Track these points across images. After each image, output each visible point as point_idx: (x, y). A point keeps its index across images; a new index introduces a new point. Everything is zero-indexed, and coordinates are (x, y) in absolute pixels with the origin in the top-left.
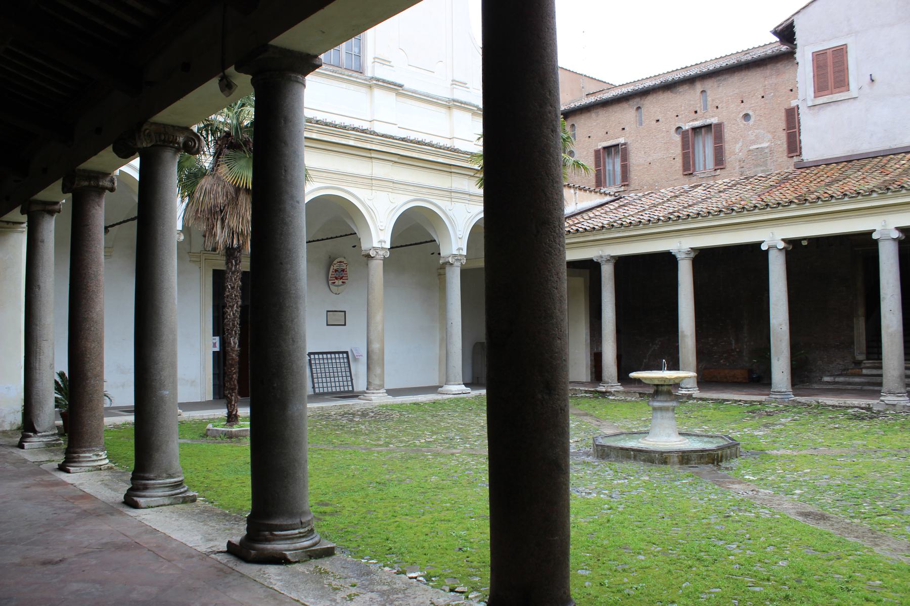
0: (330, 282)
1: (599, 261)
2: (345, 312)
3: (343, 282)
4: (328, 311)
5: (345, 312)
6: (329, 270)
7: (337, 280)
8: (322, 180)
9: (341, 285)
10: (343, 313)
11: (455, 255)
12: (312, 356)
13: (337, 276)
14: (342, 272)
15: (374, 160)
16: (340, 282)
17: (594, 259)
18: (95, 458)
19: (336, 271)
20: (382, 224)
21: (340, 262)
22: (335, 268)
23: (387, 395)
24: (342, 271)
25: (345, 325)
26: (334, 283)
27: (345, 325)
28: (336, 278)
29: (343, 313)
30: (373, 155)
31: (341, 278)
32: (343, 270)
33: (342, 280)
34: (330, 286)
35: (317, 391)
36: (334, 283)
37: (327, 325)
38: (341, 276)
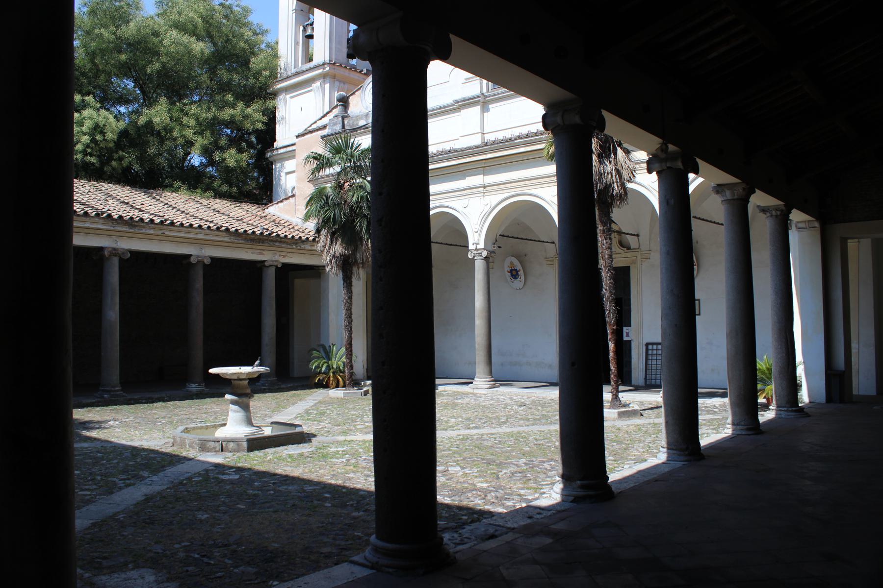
35: (648, 383)
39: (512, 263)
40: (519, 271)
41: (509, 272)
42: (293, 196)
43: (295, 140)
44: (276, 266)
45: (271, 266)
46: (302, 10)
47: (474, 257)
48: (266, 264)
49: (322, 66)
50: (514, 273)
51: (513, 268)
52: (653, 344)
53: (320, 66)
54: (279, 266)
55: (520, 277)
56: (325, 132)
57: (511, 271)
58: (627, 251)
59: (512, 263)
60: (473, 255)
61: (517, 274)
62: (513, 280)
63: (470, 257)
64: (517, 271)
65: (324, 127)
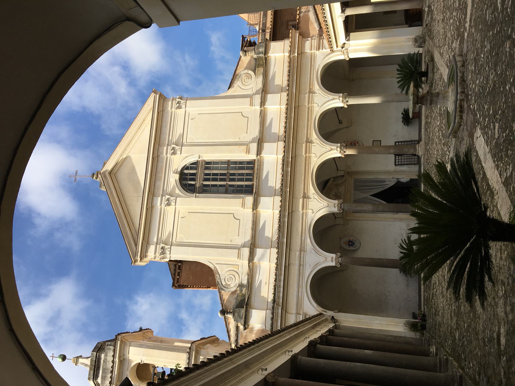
1: (345, 17)
2: (373, 141)
3: (357, 143)
5: (373, 141)
8: (309, 183)
10: (374, 142)
14: (352, 144)
15: (296, 155)
17: (343, 20)
18: (432, 354)
20: (328, 149)
23: (419, 144)
25: (380, 141)
27: (380, 141)
29: (374, 142)
33: (356, 144)
38: (354, 144)
39: (344, 243)
40: (350, 240)
41: (350, 247)
47: (342, 209)
49: (191, 350)
50: (350, 243)
51: (348, 243)
55: (353, 240)
56: (241, 327)
57: (349, 245)
58: (345, 177)
59: (344, 243)
60: (341, 209)
61: (351, 241)
62: (354, 246)
64: (349, 241)
65: (237, 328)
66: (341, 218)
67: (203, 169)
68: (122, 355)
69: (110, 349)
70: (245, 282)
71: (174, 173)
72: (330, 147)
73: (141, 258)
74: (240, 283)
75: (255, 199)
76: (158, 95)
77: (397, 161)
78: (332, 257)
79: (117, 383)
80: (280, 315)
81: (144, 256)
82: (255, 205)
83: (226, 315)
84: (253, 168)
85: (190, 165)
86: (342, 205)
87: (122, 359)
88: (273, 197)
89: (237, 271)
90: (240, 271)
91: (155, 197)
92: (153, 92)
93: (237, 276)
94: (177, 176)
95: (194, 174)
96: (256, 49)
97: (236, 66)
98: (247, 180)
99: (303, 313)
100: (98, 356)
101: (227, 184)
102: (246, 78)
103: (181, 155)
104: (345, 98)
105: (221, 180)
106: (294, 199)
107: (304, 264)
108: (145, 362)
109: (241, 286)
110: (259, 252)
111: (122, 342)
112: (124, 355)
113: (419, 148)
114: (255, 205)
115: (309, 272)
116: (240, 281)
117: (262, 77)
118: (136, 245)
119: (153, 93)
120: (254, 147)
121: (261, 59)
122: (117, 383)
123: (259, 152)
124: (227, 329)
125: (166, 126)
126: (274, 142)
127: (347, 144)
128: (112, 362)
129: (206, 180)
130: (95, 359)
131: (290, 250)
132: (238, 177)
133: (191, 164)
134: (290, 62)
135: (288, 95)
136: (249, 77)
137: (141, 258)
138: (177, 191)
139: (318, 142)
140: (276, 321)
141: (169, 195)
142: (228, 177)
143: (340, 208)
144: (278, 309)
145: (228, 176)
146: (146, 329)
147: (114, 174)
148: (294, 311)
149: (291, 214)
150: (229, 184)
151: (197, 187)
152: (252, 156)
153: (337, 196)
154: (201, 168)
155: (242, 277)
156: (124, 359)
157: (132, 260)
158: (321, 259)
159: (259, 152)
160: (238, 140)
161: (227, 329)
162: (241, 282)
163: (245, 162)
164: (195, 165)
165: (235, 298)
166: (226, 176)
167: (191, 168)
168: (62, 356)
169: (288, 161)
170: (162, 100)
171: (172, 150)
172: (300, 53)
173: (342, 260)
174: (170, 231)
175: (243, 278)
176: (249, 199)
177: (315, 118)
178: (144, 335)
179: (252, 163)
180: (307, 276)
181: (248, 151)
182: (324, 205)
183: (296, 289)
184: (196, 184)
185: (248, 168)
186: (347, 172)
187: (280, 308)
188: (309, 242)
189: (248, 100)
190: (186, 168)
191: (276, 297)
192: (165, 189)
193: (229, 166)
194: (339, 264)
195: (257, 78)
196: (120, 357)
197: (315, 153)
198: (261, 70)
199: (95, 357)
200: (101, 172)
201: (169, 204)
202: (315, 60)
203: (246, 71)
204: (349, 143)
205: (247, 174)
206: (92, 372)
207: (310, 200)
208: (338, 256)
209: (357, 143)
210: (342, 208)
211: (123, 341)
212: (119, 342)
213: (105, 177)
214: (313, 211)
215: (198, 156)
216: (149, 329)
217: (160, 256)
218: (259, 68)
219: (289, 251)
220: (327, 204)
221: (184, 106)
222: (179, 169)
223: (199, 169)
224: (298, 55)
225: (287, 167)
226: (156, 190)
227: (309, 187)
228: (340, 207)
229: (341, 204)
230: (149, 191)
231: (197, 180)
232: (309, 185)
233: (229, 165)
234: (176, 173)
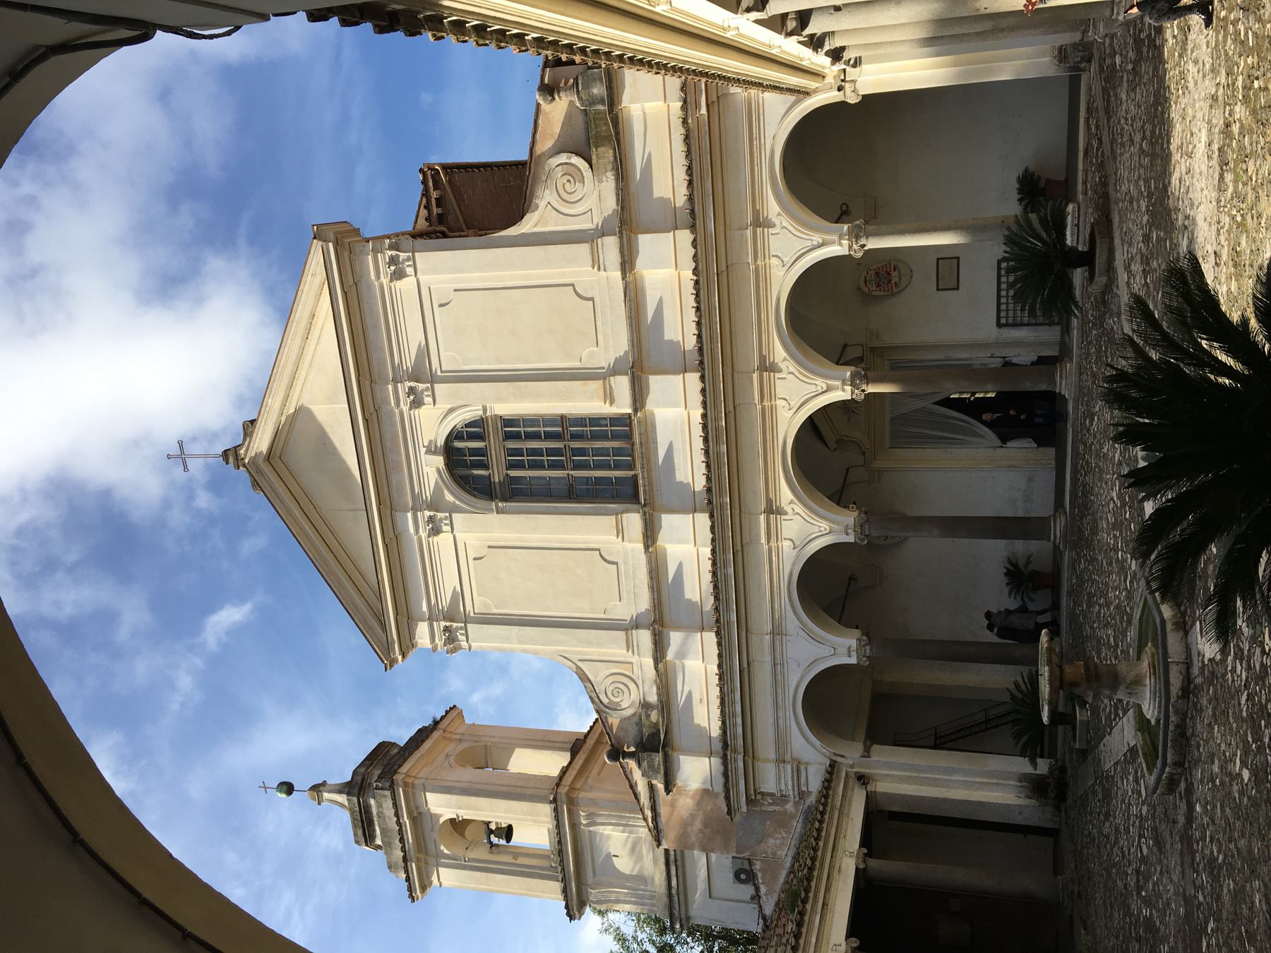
0: (895, 290)
2: (938, 259)
3: (894, 270)
4: (938, 289)
5: (938, 259)
6: (879, 296)
7: (891, 281)
9: (900, 272)
11: (850, 247)
12: (1003, 321)
13: (886, 282)
14: (881, 276)
15: (737, 403)
16: (894, 274)
19: (878, 285)
20: (819, 388)
21: (866, 282)
22: (874, 288)
24: (878, 276)
25: (958, 258)
26: (895, 283)
27: (958, 258)
28: (890, 281)
30: (731, 408)
31: (889, 274)
32: (877, 274)
34: (900, 288)
36: (895, 283)
37: (958, 288)
38: (886, 275)
42: (750, 862)
43: (661, 851)
44: (866, 855)
45: (864, 862)
46: (467, 849)
48: (861, 867)
52: (998, 317)
53: (556, 810)
54: (866, 851)
56: (660, 786)
63: (866, 542)
65: (651, 788)
66: (861, 466)
67: (501, 439)
68: (414, 809)
69: (385, 796)
70: (653, 698)
71: (429, 452)
72: (826, 383)
73: (403, 653)
74: (642, 700)
75: (648, 521)
76: (331, 245)
77: (1003, 314)
78: (849, 647)
79: (419, 855)
80: (741, 771)
81: (408, 647)
82: (650, 534)
83: (621, 760)
84: (628, 437)
85: (466, 427)
86: (866, 526)
87: (416, 815)
88: (672, 232)
89: (631, 674)
90: (637, 674)
91: (377, 385)
92: (315, 238)
93: (632, 685)
94: (439, 461)
95: (481, 452)
96: (580, 89)
97: (531, 135)
98: (618, 466)
99: (793, 760)
100: (363, 803)
101: (570, 477)
102: (569, 181)
103: (436, 406)
104: (857, 238)
105: (553, 466)
106: (743, 516)
107: (785, 662)
108: (465, 817)
109: (646, 706)
110: (675, 638)
111: (406, 785)
112: (417, 808)
113: (1064, 382)
114: (650, 534)
115: (797, 679)
116: (642, 696)
117: (613, 177)
118: (384, 627)
119: (315, 241)
120: (622, 385)
121: (602, 119)
122: (419, 855)
123: (639, 397)
124: (629, 781)
125: (377, 326)
126: (674, 372)
127: (865, 277)
128: (402, 851)
129: (512, 466)
130: (358, 809)
131: (747, 632)
132: (594, 458)
133: (467, 426)
134: (687, 139)
135: (702, 378)
136: (574, 175)
137: (403, 653)
138: (449, 497)
139: (792, 369)
140: (735, 784)
141: (430, 508)
142: (569, 460)
143: (861, 534)
144: (736, 760)
145: (568, 456)
146: (447, 712)
147: (278, 455)
148: (772, 756)
149: (740, 554)
150: (571, 446)
151: (494, 482)
152: (623, 407)
153: (851, 411)
154: (496, 437)
155: (643, 687)
156: (420, 813)
157: (383, 662)
158: (824, 651)
159: (639, 397)
160: (577, 364)
161: (629, 781)
162: (644, 699)
163: (605, 419)
164: (476, 429)
165: (636, 723)
166: (563, 456)
167: (472, 437)
168: (285, 788)
169: (726, 576)
170: (346, 254)
171: (409, 397)
172: (715, 99)
173: (871, 650)
174: (455, 588)
175: (646, 689)
176: (634, 521)
177: (778, 300)
178: (445, 735)
179: (624, 420)
180: (793, 685)
181: (610, 397)
182: (821, 529)
183: (770, 711)
184: (492, 476)
185: (615, 436)
186: (870, 348)
187: (740, 757)
188: (794, 619)
189: (584, 249)
190: (454, 435)
191: (729, 738)
192: (416, 491)
193: (565, 431)
194: (865, 659)
195: (600, 181)
196: (410, 813)
197: (787, 398)
198: (605, 154)
199: (357, 805)
200: (246, 461)
201: (436, 531)
202: (761, 117)
203: (563, 158)
204: (873, 272)
205: (617, 452)
206: (360, 832)
207: (783, 517)
208: (863, 643)
209: (894, 270)
210: (867, 533)
211: (408, 783)
212: (401, 789)
213: (259, 471)
214: (794, 544)
215: (481, 408)
216: (451, 709)
217: (445, 648)
218: (599, 149)
219: (747, 635)
220: (827, 527)
221: (410, 270)
222: (441, 442)
223: (489, 436)
224: (710, 107)
225: (717, 443)
226: (395, 495)
227: (778, 486)
228: (860, 527)
229: (861, 526)
230: (379, 504)
231: (490, 466)
232: (777, 481)
233: (565, 427)
234: (435, 453)
